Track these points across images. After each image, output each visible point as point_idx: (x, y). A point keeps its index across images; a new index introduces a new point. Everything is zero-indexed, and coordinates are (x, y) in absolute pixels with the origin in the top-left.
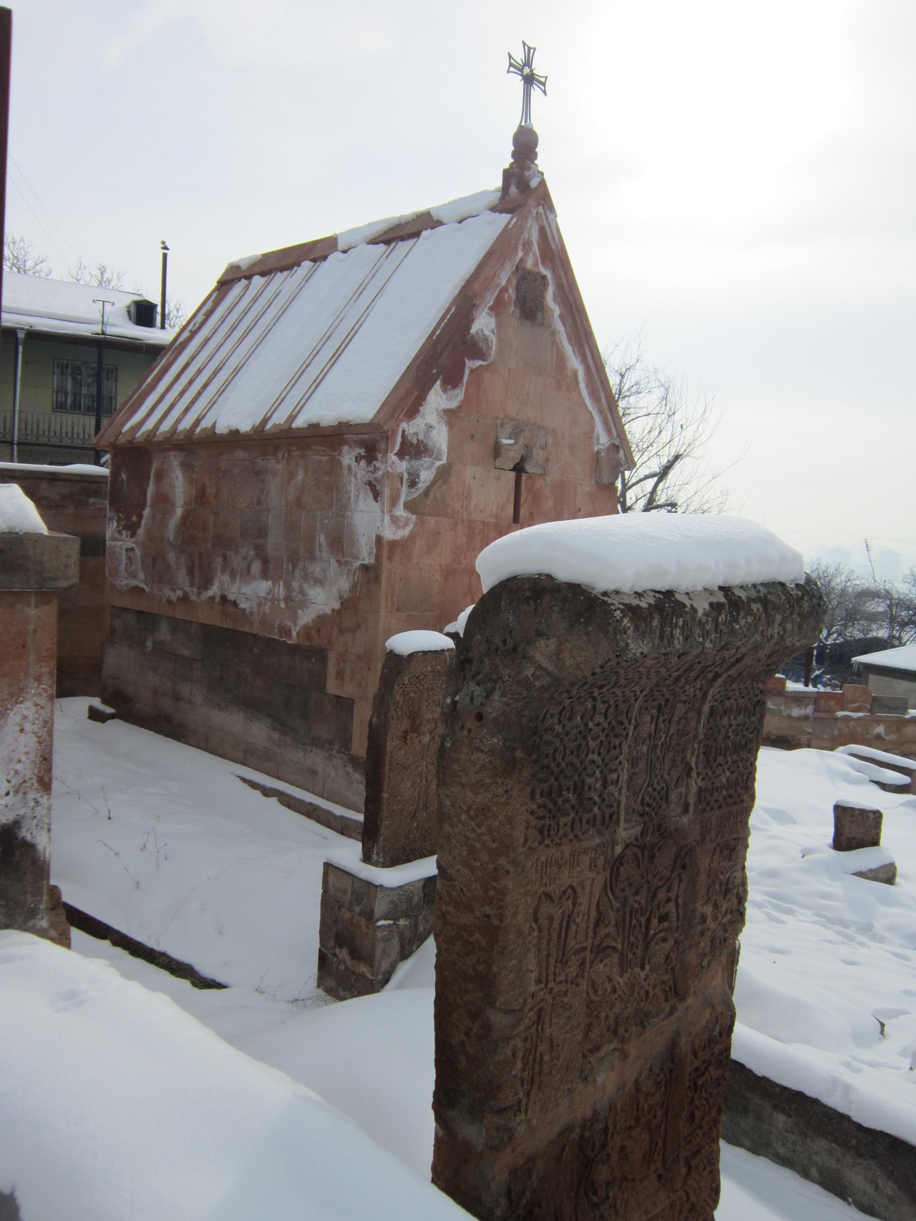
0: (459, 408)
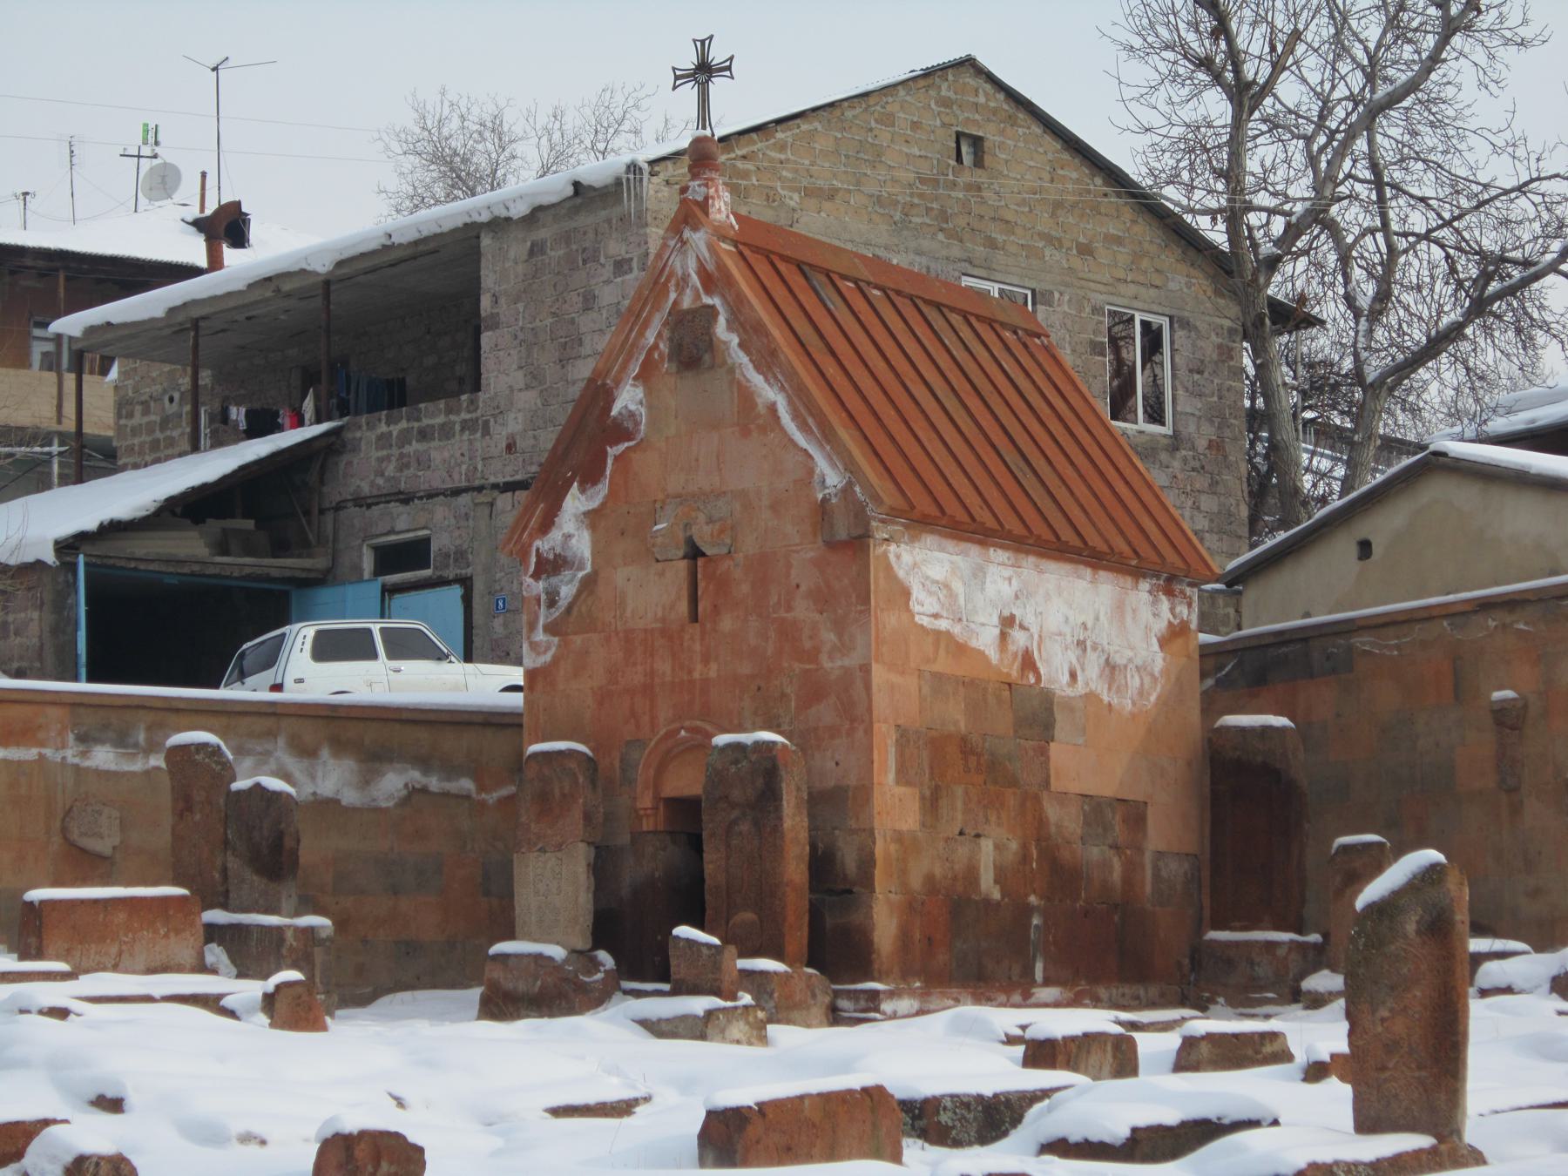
0: (603, 505)
